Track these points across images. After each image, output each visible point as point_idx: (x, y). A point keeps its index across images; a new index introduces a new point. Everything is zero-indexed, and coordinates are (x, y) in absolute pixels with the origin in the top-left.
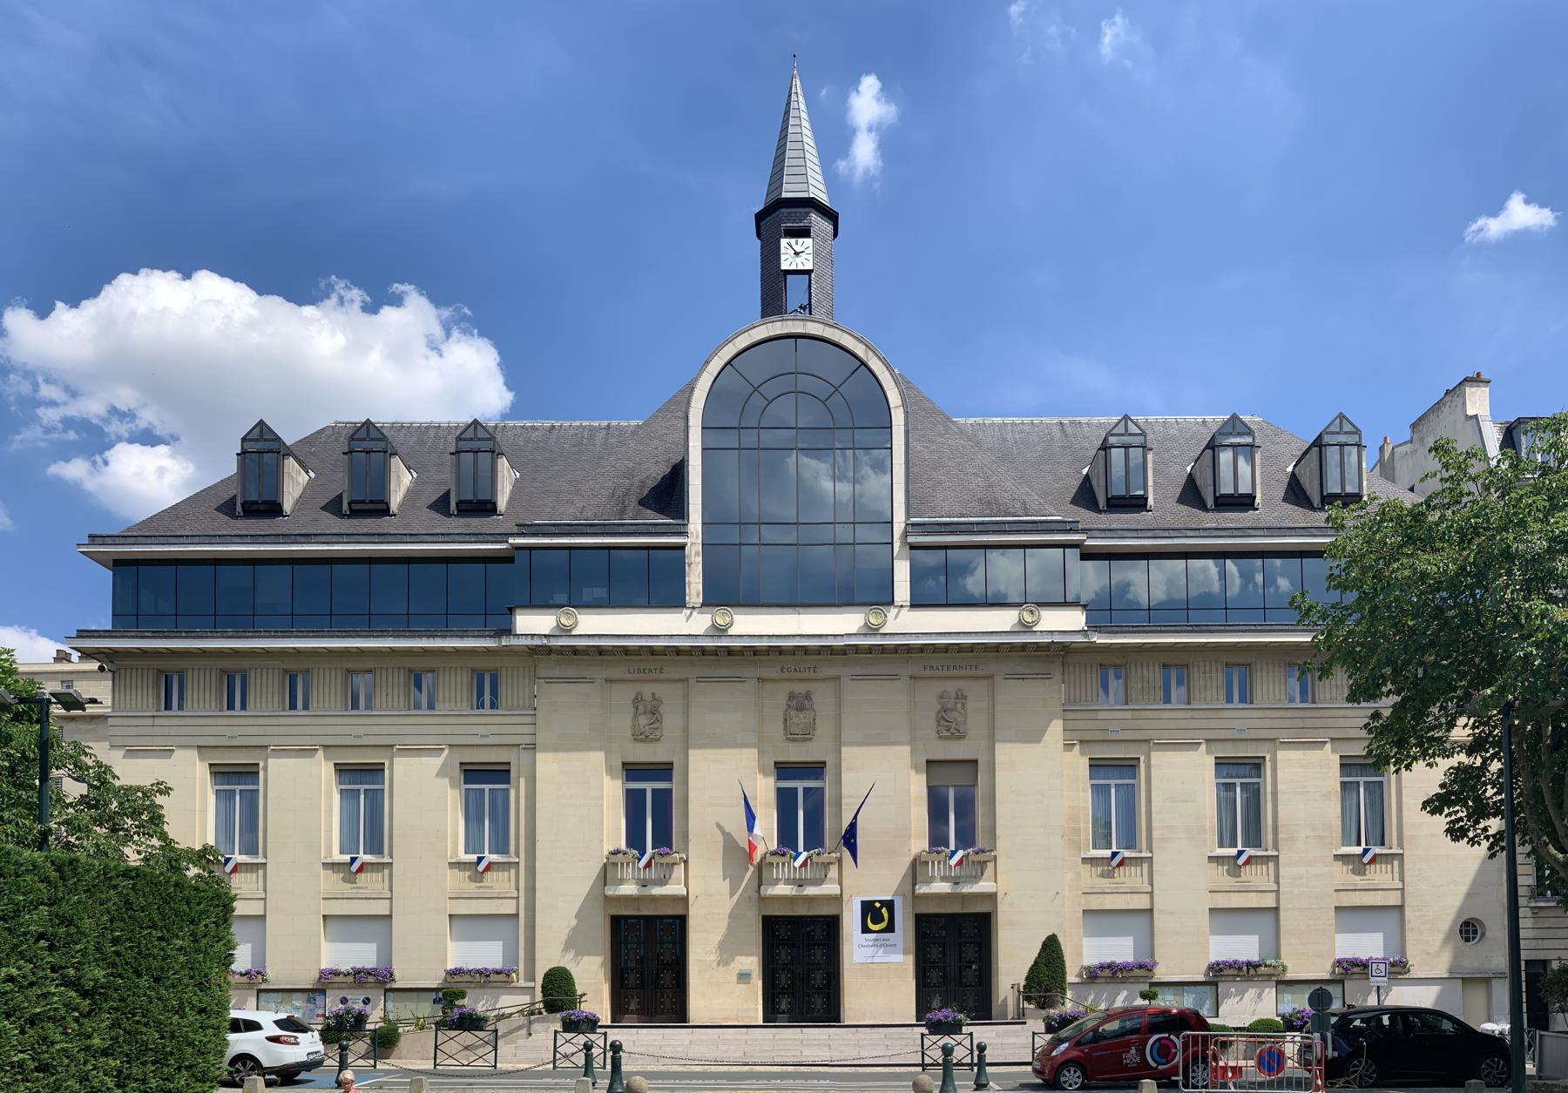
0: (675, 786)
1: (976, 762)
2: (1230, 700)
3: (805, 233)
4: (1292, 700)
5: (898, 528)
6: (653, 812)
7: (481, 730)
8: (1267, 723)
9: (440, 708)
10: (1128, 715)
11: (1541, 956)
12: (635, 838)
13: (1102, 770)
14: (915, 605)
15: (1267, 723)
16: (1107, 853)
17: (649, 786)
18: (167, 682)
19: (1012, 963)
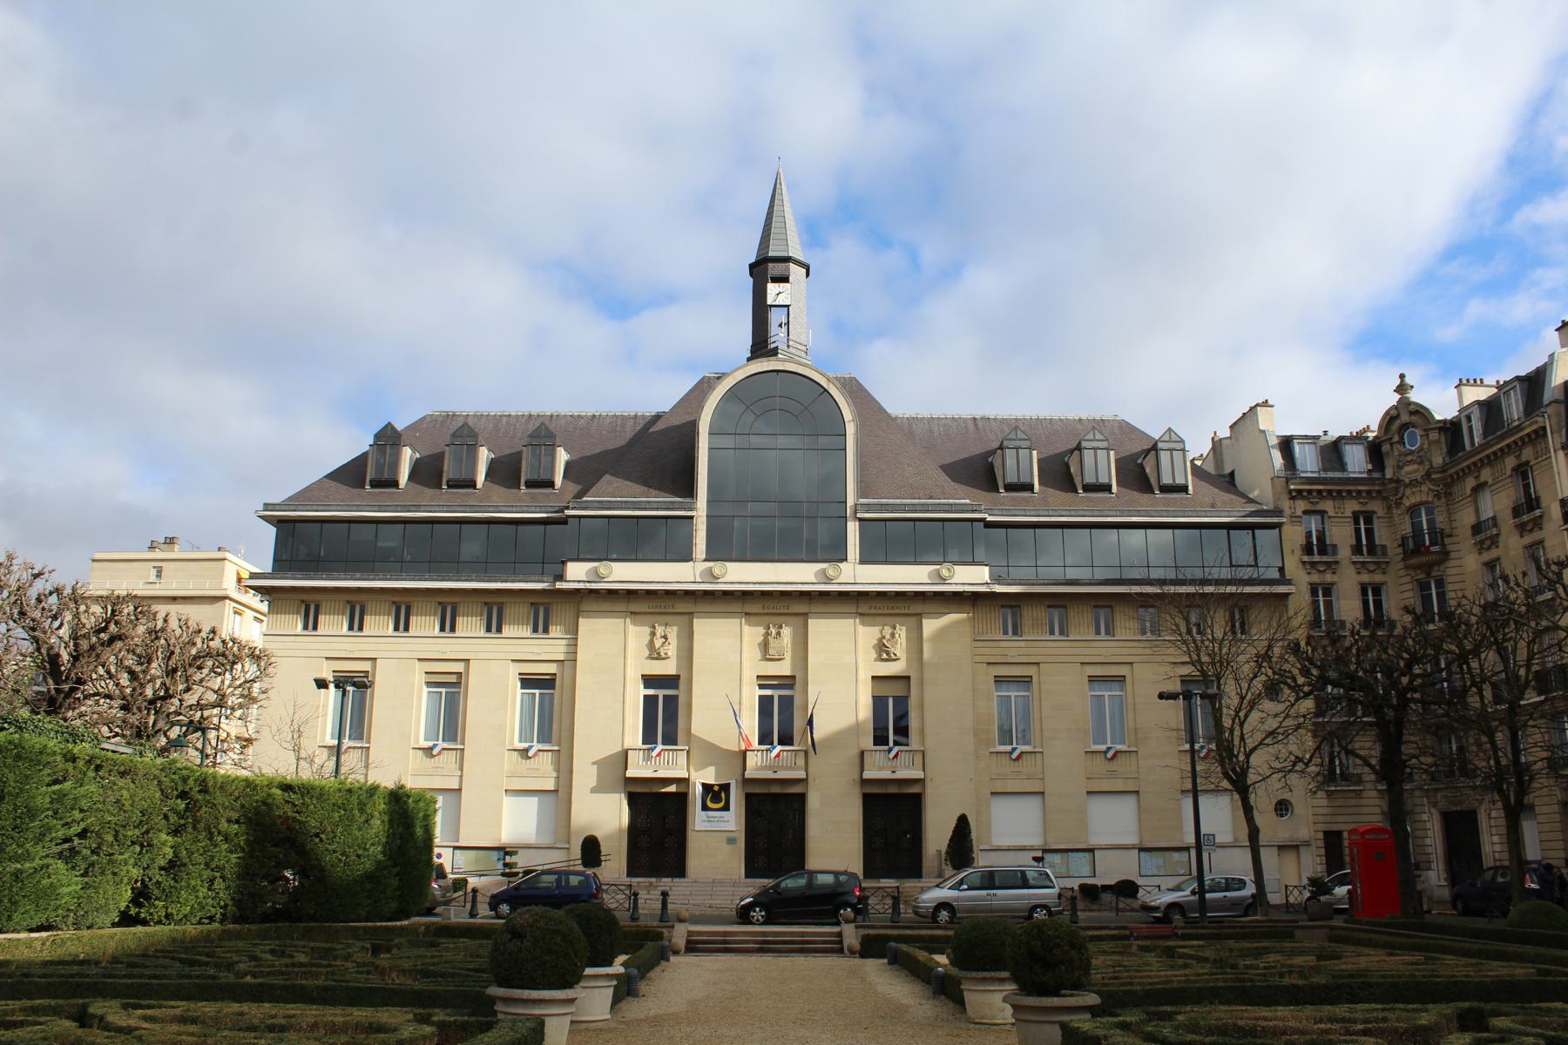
0: (681, 693)
1: (908, 678)
2: (1098, 633)
3: (785, 279)
4: (1144, 633)
5: (851, 501)
6: (665, 711)
7: (535, 649)
8: (1125, 651)
9: (508, 630)
10: (1022, 644)
11: (1335, 828)
12: (649, 737)
13: (1004, 686)
14: (865, 560)
15: (1125, 651)
16: (1009, 748)
17: (661, 693)
18: (310, 607)
19: (936, 836)
